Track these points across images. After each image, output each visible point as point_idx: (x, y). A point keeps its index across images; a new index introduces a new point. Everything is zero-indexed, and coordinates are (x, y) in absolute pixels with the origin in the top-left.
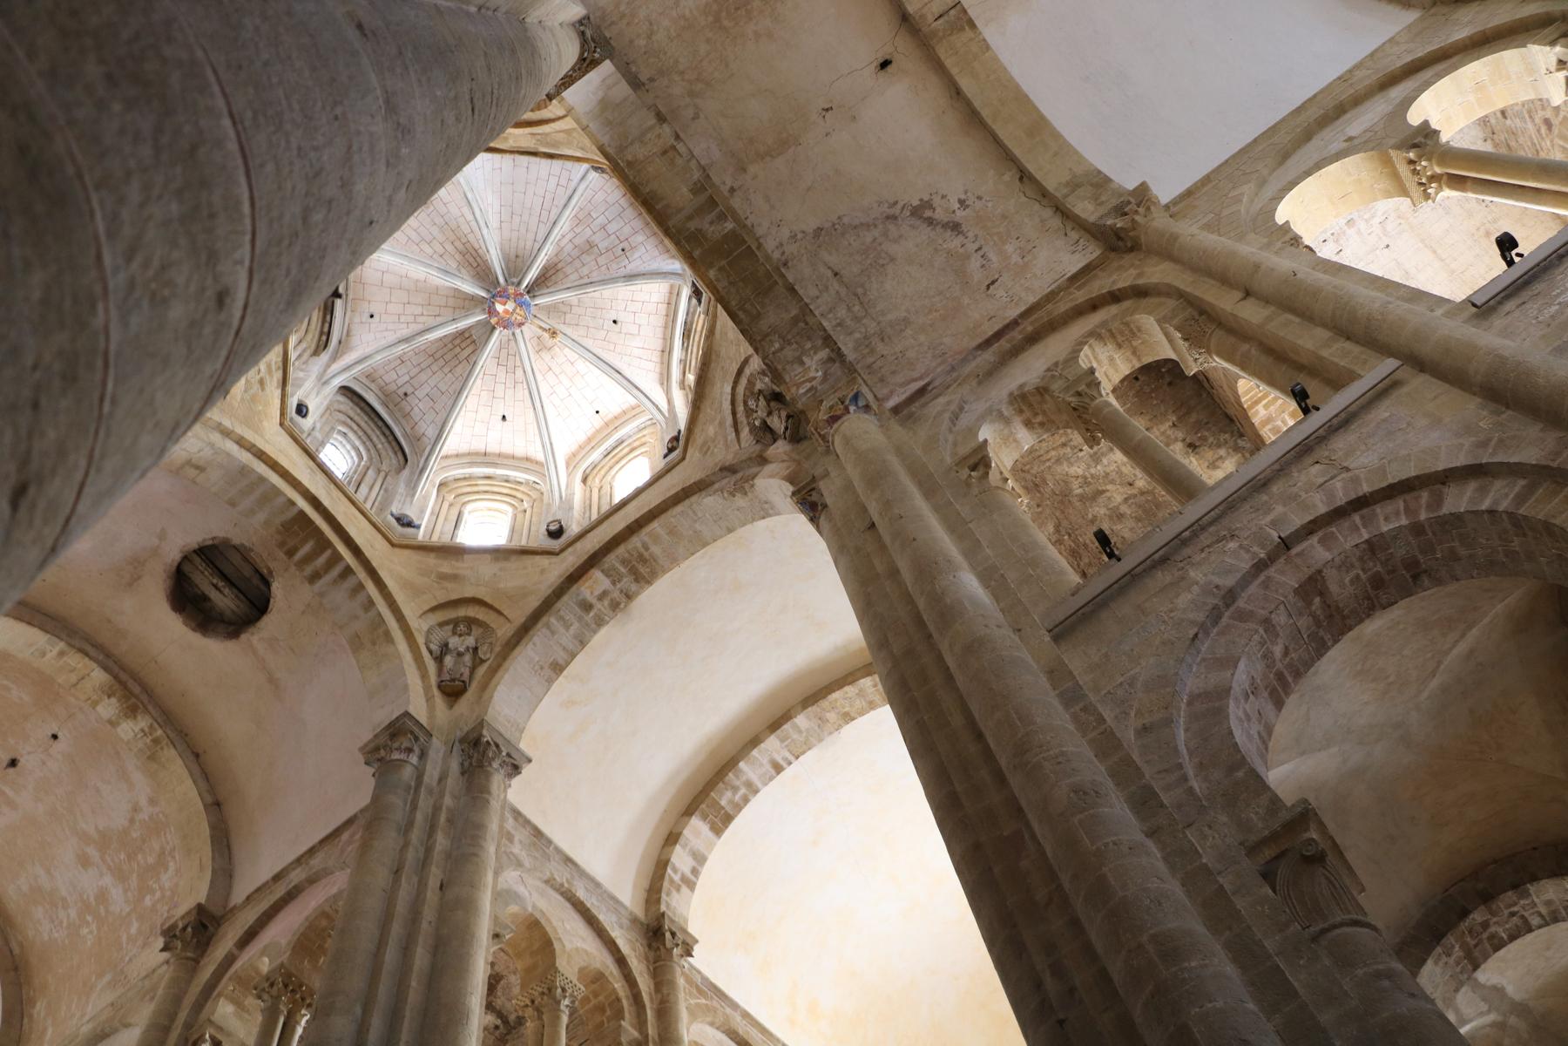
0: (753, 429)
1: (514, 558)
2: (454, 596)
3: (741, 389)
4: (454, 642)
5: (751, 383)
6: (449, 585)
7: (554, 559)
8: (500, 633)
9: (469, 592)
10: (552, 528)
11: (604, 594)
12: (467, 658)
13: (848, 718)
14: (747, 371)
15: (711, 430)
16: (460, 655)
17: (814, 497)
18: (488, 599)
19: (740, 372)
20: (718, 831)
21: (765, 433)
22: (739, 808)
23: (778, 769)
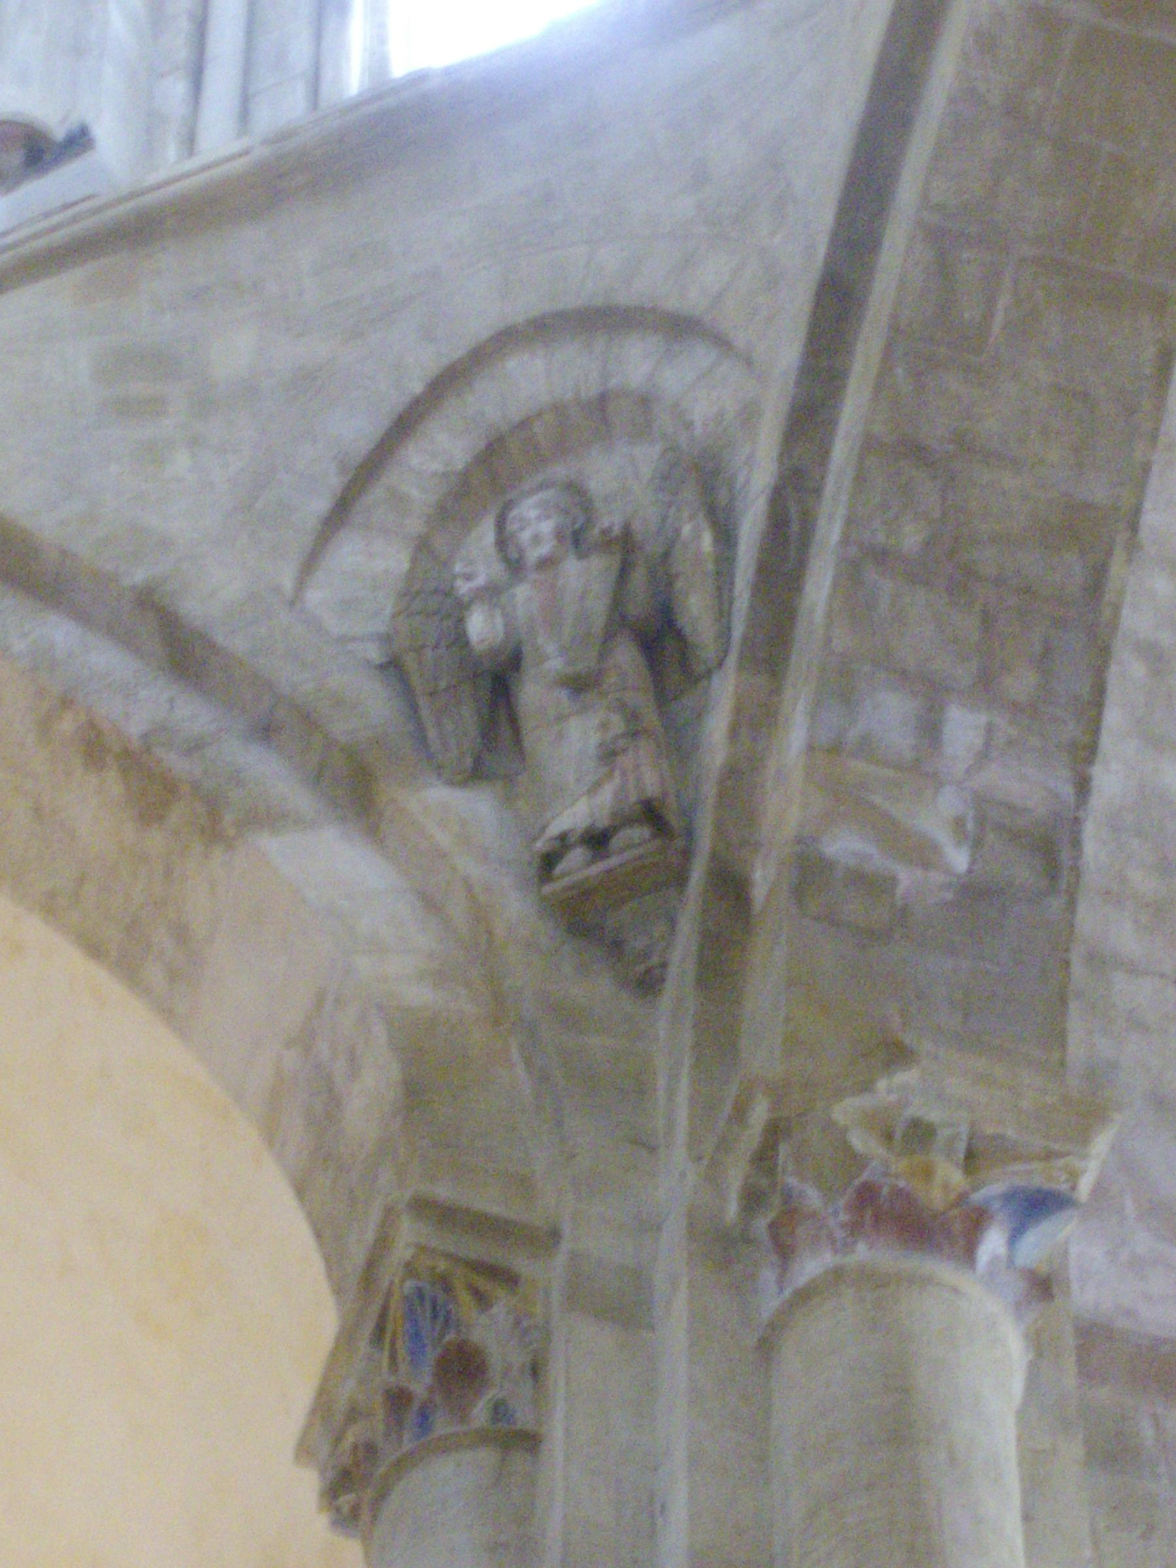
0: (431, 600)
3: (531, 381)
5: (602, 415)
14: (636, 361)
15: (236, 350)
17: (489, 1330)
19: (602, 320)
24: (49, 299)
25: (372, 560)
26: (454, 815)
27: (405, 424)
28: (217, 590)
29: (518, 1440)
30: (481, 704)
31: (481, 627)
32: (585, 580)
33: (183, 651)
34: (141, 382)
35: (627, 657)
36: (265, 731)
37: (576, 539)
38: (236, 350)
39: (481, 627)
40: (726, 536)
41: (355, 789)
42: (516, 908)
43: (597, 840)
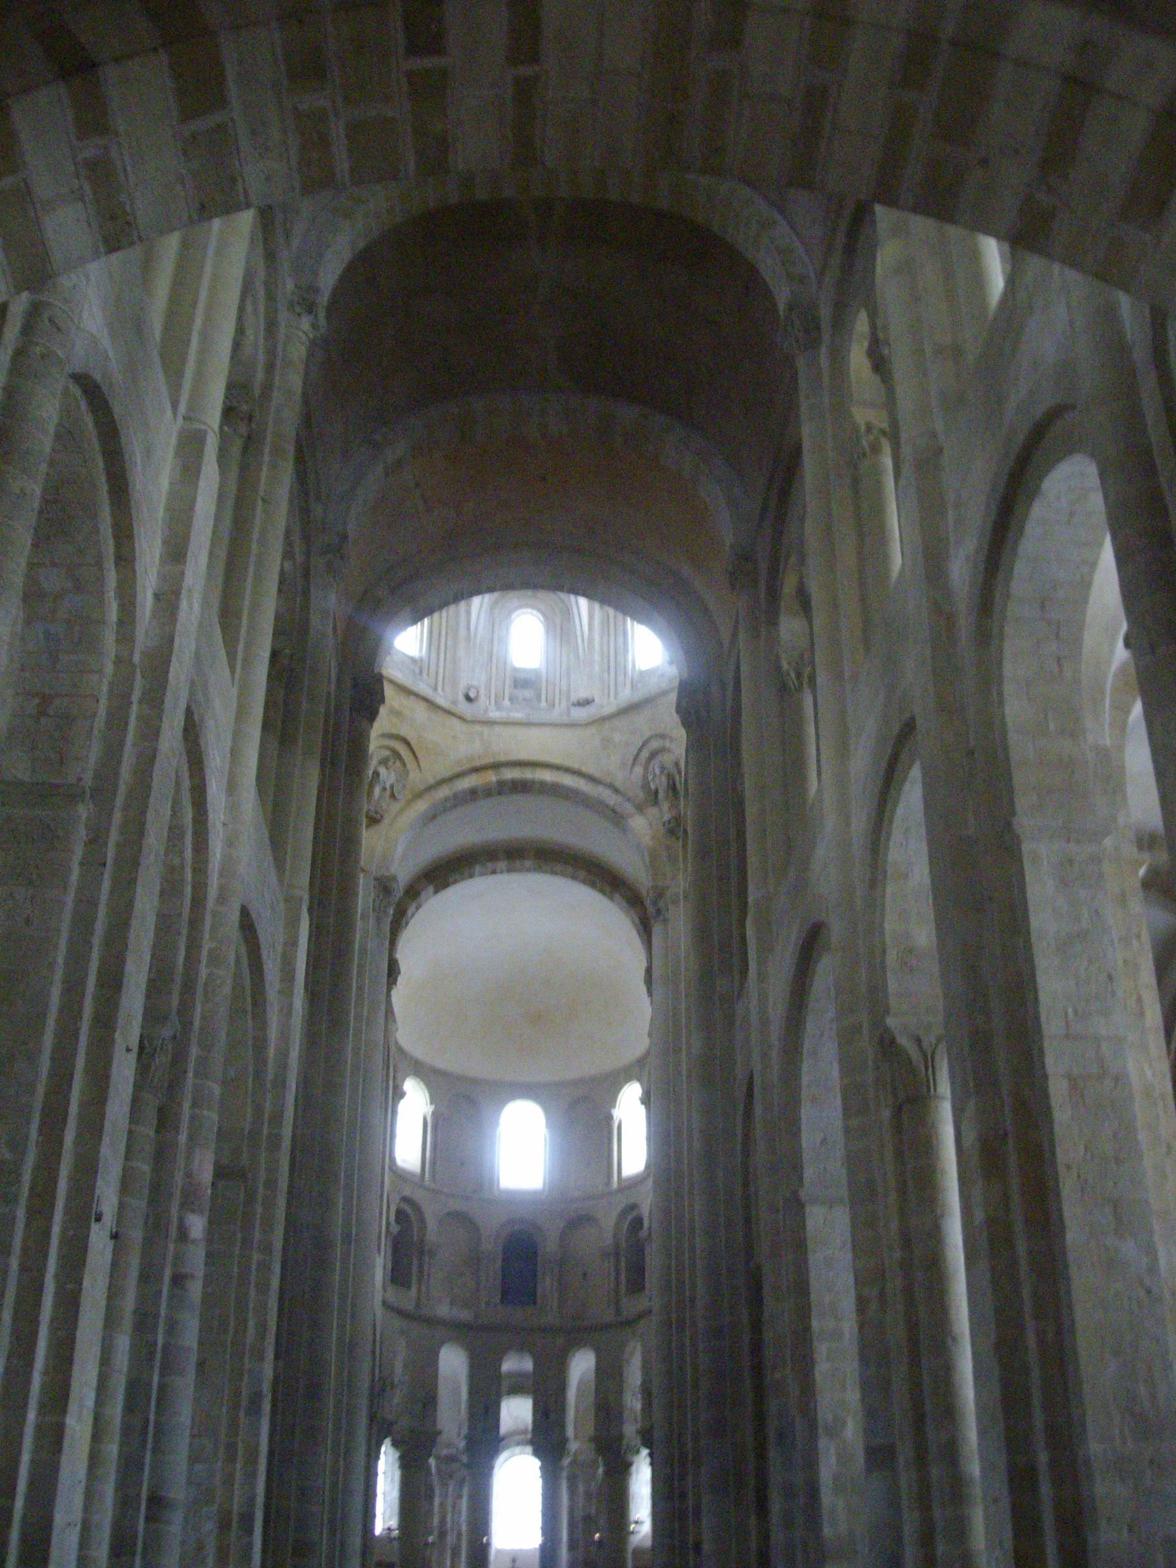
0: (645, 777)
1: (440, 712)
2: (394, 731)
3: (655, 744)
4: (382, 770)
6: (394, 720)
7: (465, 727)
8: (411, 776)
9: (403, 732)
10: (472, 695)
11: (490, 789)
12: (388, 793)
13: (553, 873)
16: (384, 789)
17: (661, 904)
18: (413, 743)
19: (663, 736)
20: (436, 892)
21: (654, 797)
22: (455, 882)
23: (494, 872)
24: (593, 730)
25: (639, 770)
26: (652, 811)
27: (640, 750)
28: (619, 779)
29: (665, 921)
30: (654, 797)
31: (653, 786)
32: (664, 779)
33: (617, 791)
34: (606, 742)
35: (670, 792)
36: (629, 800)
37: (662, 772)
38: (617, 737)
39: (653, 786)
40: (679, 772)
41: (640, 808)
42: (662, 831)
43: (669, 822)
